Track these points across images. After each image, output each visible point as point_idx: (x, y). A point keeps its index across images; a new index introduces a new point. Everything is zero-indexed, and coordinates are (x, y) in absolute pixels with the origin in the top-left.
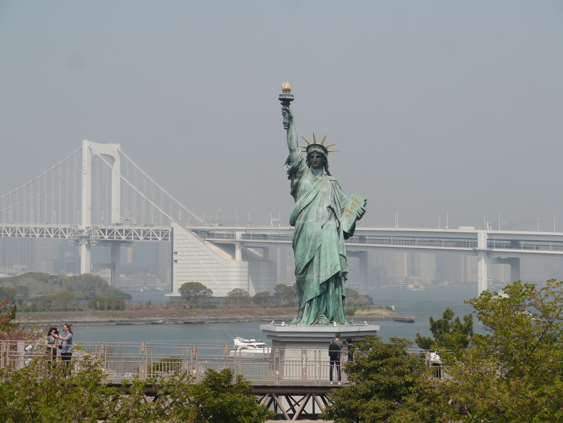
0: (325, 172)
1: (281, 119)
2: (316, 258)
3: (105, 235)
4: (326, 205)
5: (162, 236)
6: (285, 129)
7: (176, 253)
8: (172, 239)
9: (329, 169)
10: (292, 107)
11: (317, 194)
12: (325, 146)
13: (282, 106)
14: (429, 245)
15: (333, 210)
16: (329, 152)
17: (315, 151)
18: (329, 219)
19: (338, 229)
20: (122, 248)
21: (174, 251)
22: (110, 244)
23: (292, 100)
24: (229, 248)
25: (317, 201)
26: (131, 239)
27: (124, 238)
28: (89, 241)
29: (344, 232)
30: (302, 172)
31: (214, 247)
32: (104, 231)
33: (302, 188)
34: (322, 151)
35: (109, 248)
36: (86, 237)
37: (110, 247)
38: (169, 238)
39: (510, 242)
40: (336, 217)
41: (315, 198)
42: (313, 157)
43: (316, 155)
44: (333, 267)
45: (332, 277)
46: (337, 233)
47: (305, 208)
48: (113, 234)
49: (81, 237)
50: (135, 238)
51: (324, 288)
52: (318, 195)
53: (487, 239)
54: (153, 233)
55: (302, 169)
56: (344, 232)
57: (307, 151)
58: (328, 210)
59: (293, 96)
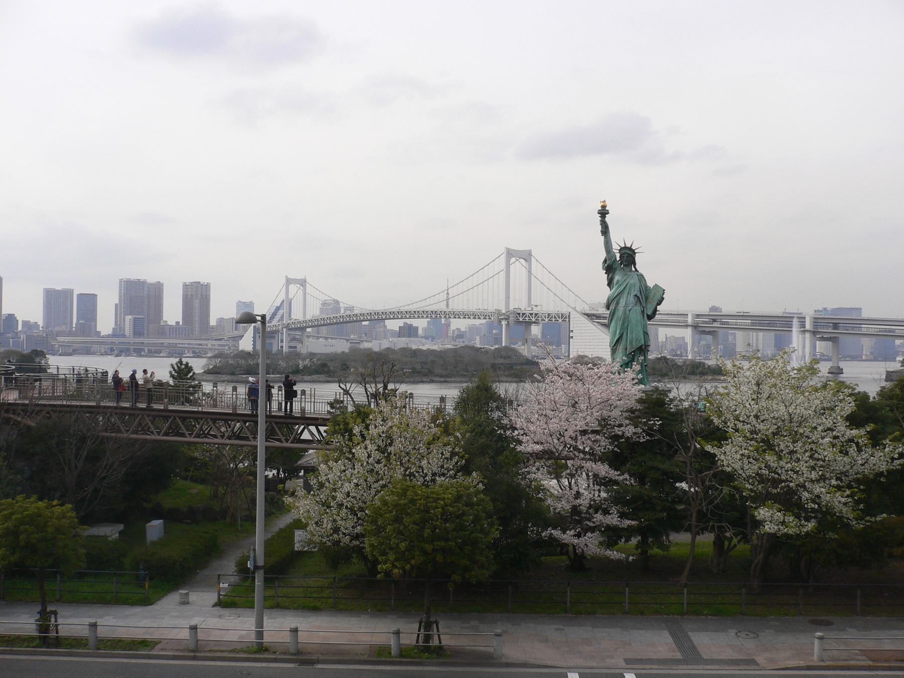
0: (633, 269)
1: (599, 228)
2: (625, 334)
3: (520, 317)
4: (633, 294)
5: (562, 318)
6: (602, 235)
7: (572, 331)
8: (569, 321)
9: (636, 266)
10: (608, 218)
11: (626, 285)
12: (633, 248)
13: (600, 219)
14: (767, 326)
15: (638, 297)
16: (637, 254)
17: (625, 253)
18: (636, 304)
19: (643, 312)
21: (571, 329)
22: (524, 324)
23: (608, 213)
25: (626, 292)
26: (539, 320)
27: (534, 320)
28: (508, 322)
29: (647, 314)
30: (615, 269)
33: (615, 281)
34: (631, 253)
35: (522, 327)
38: (567, 320)
39: (831, 325)
40: (641, 304)
41: (624, 289)
42: (624, 257)
43: (626, 255)
44: (638, 342)
45: (638, 349)
46: (642, 316)
47: (616, 296)
49: (502, 319)
50: (542, 320)
51: (630, 357)
52: (627, 287)
53: (814, 322)
54: (555, 316)
55: (615, 267)
56: (647, 314)
57: (619, 252)
58: (635, 298)
59: (608, 211)
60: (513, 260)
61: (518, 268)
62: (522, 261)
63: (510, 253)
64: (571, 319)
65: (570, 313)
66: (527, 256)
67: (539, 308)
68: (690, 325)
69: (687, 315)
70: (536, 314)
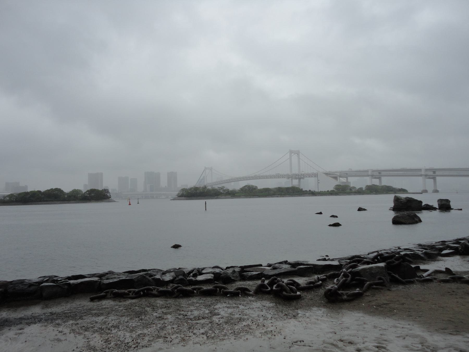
7: (319, 180)
20: (302, 180)
24: (336, 178)
27: (302, 177)
31: (330, 178)
32: (296, 175)
36: (291, 177)
37: (298, 180)
48: (299, 176)
60: (293, 154)
61: (295, 158)
62: (296, 154)
63: (291, 152)
64: (318, 176)
65: (317, 173)
66: (298, 153)
67: (303, 172)
68: (370, 175)
69: (368, 171)
70: (303, 175)
